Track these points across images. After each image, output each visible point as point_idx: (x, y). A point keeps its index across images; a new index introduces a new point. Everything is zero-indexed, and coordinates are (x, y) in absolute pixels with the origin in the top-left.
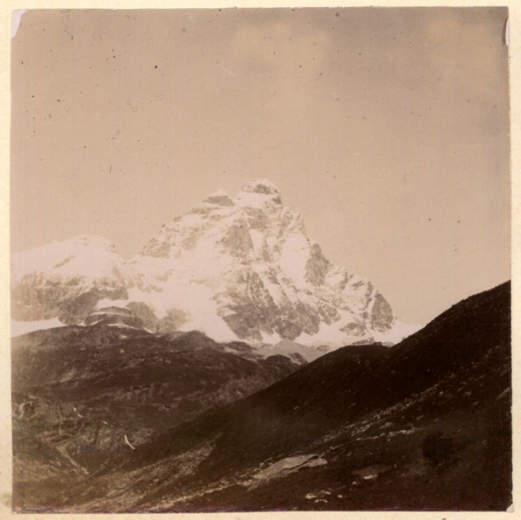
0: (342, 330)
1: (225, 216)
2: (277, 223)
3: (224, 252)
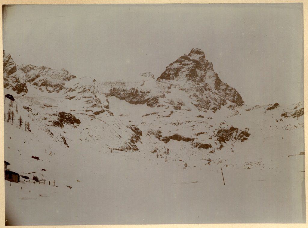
0: (228, 108)
2: (203, 66)
3: (190, 79)
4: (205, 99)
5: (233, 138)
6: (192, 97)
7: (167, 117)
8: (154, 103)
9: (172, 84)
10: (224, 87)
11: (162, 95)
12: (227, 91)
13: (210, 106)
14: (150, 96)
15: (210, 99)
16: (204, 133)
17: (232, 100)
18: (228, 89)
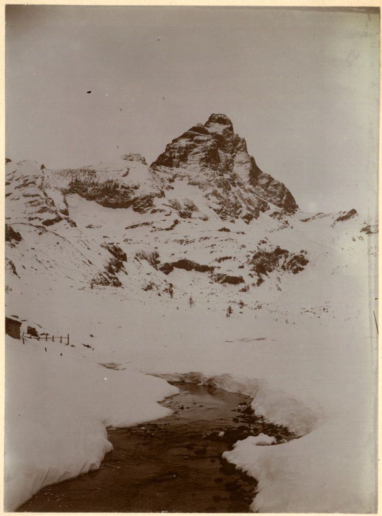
0: (271, 216)
1: (204, 141)
2: (231, 144)
3: (207, 166)
4: (233, 200)
5: (280, 267)
6: (210, 196)
7: (167, 229)
8: (146, 207)
9: (176, 175)
10: (264, 181)
11: (159, 192)
12: (270, 187)
13: (241, 212)
14: (138, 194)
15: (241, 201)
16: (230, 258)
17: (279, 203)
18: (271, 184)
